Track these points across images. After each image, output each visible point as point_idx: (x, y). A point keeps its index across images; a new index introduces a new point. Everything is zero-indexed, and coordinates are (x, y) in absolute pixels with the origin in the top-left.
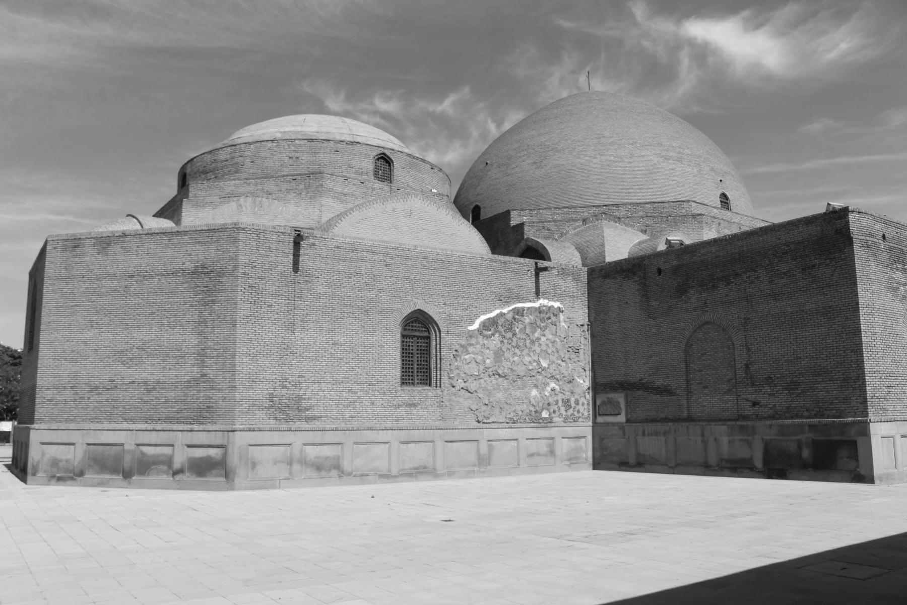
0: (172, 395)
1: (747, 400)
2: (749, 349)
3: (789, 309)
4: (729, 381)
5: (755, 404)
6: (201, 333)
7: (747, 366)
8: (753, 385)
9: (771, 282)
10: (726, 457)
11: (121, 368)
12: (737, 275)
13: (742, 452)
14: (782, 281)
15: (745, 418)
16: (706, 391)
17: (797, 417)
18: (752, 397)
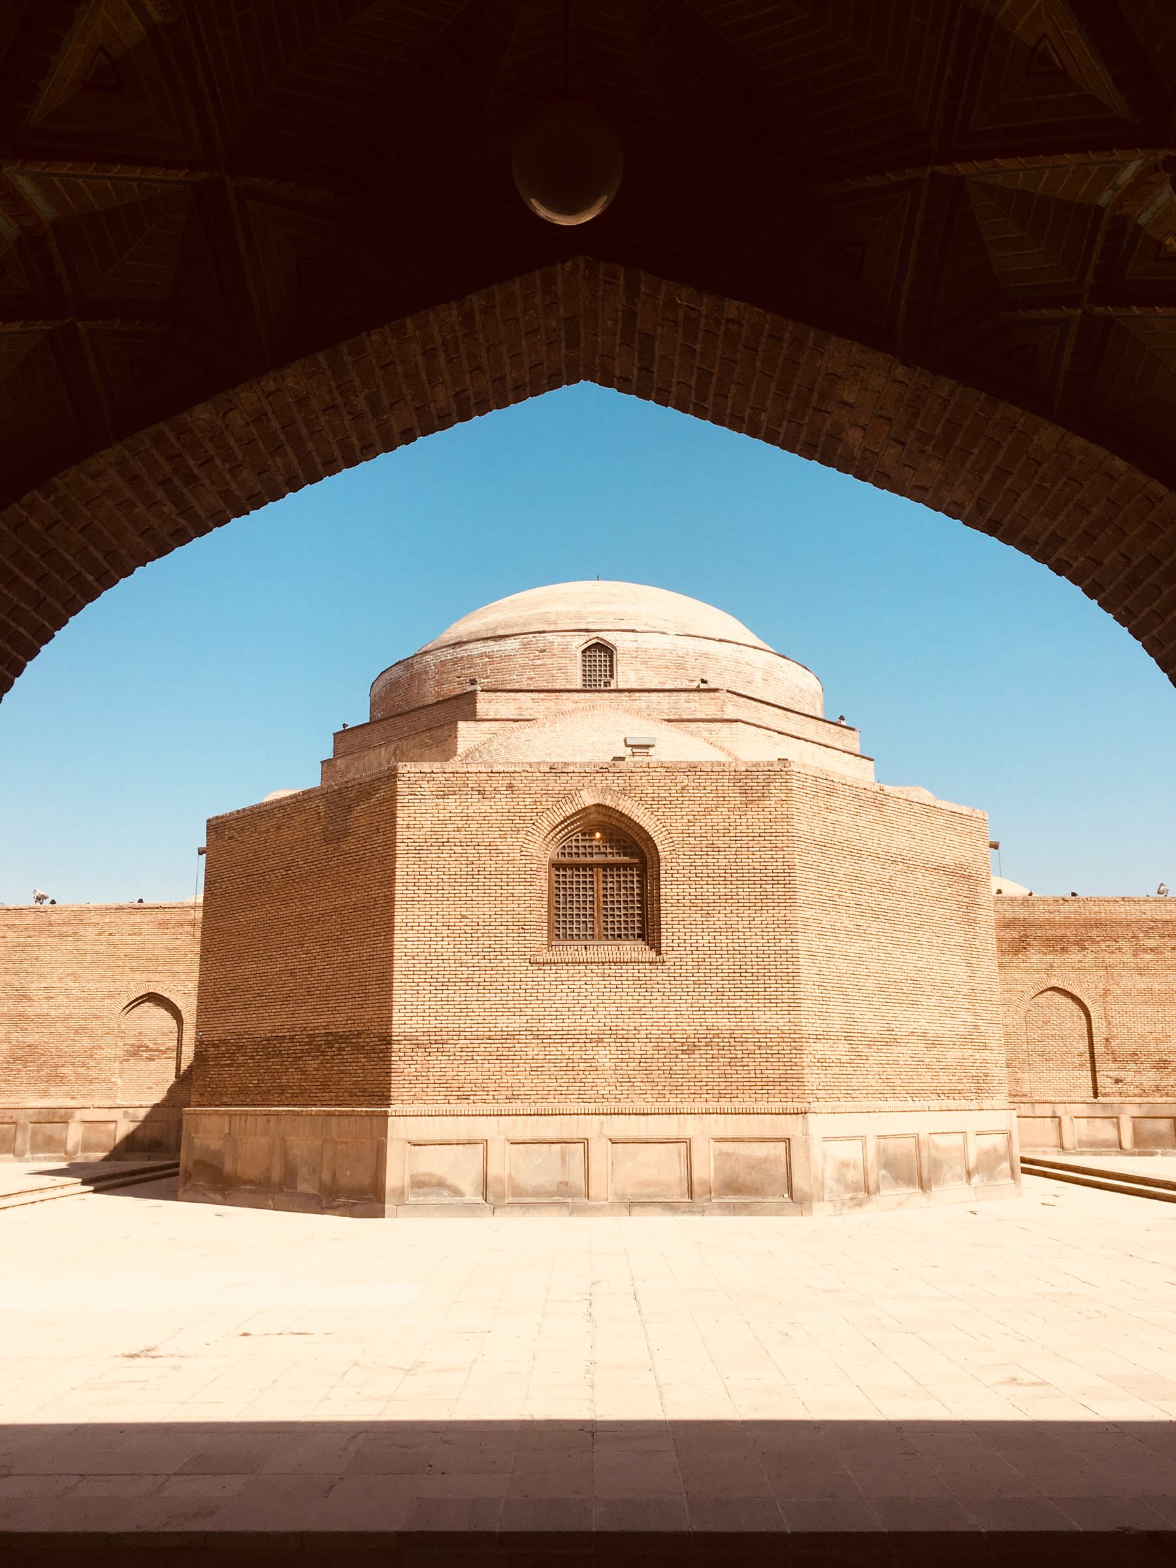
0: (953, 1054)
1: (1108, 1077)
2: (1109, 1023)
3: (1157, 987)
4: (1080, 1055)
5: (1117, 1081)
6: (969, 964)
7: (1107, 1040)
8: (1115, 1060)
9: (1135, 956)
10: (1084, 1138)
11: (898, 1009)
12: (1093, 942)
13: (1105, 1131)
14: (1148, 957)
15: (1105, 1095)
16: (1051, 1064)
17: (1167, 1095)
18: (1114, 1074)
